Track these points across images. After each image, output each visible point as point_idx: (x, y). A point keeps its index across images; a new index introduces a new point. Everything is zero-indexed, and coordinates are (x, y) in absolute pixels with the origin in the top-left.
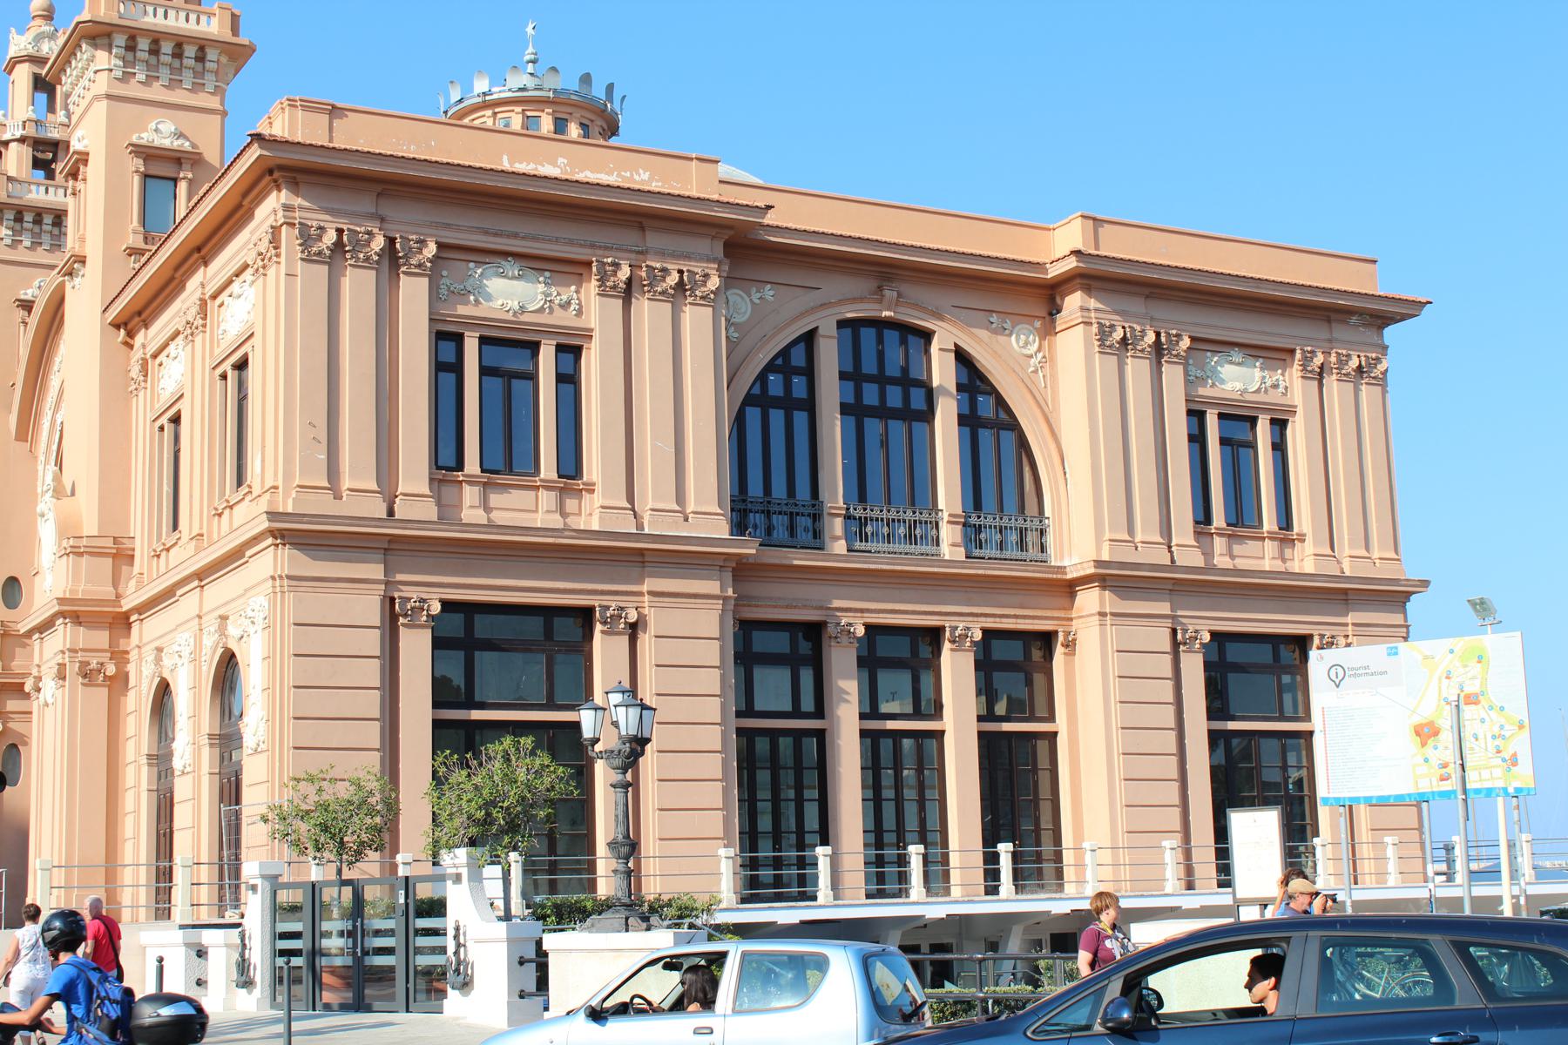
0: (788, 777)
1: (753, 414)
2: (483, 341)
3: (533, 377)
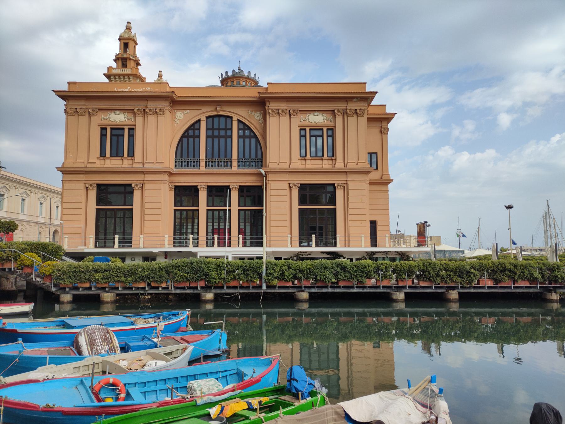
0: (216, 220)
1: (185, 140)
2: (112, 129)
3: (123, 136)
